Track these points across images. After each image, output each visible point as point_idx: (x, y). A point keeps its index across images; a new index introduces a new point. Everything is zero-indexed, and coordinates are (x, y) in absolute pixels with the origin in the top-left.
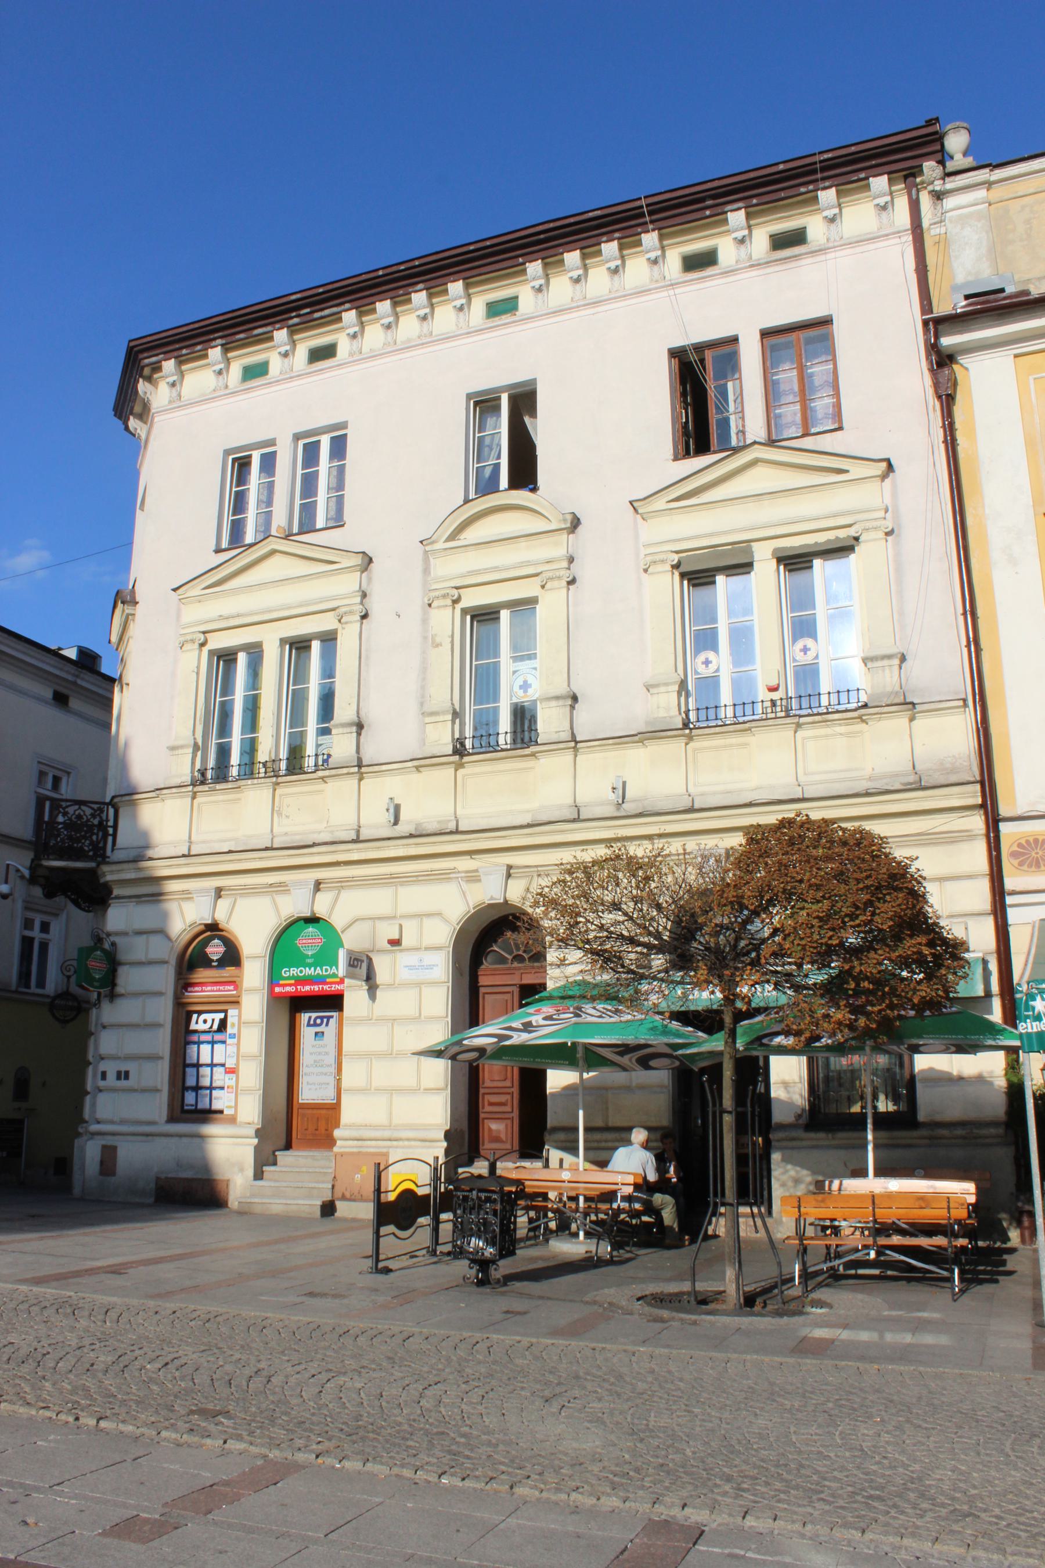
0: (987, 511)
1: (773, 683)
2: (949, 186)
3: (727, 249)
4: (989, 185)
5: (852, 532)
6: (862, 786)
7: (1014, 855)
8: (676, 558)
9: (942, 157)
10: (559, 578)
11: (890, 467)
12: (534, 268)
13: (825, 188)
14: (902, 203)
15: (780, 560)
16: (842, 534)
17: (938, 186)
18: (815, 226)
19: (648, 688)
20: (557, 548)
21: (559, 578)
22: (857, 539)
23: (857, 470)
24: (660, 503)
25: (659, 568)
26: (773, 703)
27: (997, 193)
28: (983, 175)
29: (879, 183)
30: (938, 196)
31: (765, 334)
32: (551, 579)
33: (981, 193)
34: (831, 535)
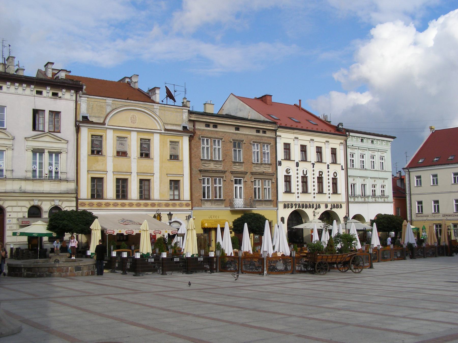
0: (81, 152)
1: (47, 174)
2: (83, 96)
3: (44, 92)
4: (88, 98)
5: (61, 151)
6: (59, 192)
7: (80, 204)
8: (32, 149)
9: (82, 91)
10: (11, 148)
11: (68, 142)
12: (9, 83)
13: (64, 89)
14: (75, 95)
15: (49, 153)
16: (59, 151)
17: (81, 95)
18: (60, 94)
19: (26, 171)
20: (10, 142)
21: (11, 148)
22: (61, 152)
23: (63, 141)
24: (30, 139)
25: (29, 150)
26: (46, 177)
27: (89, 99)
28: (88, 96)
29: (73, 91)
30: (80, 97)
31: (50, 111)
32: (9, 148)
33: (86, 99)
34: (57, 151)
